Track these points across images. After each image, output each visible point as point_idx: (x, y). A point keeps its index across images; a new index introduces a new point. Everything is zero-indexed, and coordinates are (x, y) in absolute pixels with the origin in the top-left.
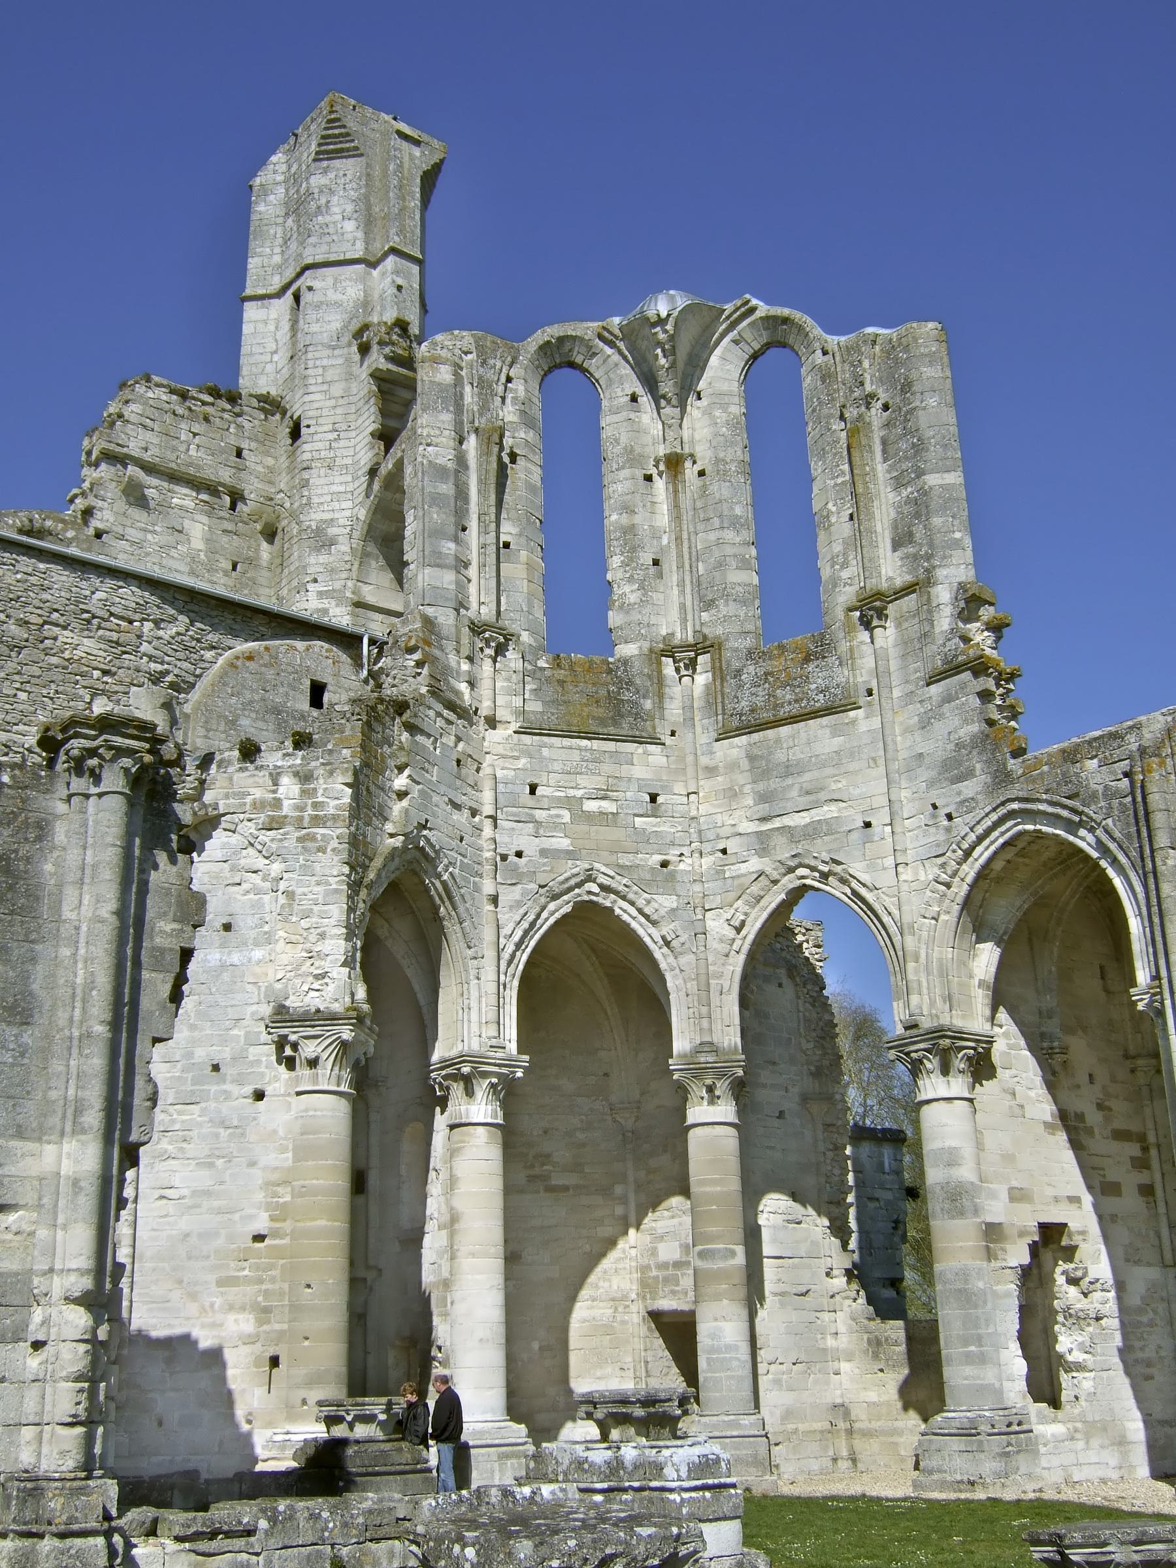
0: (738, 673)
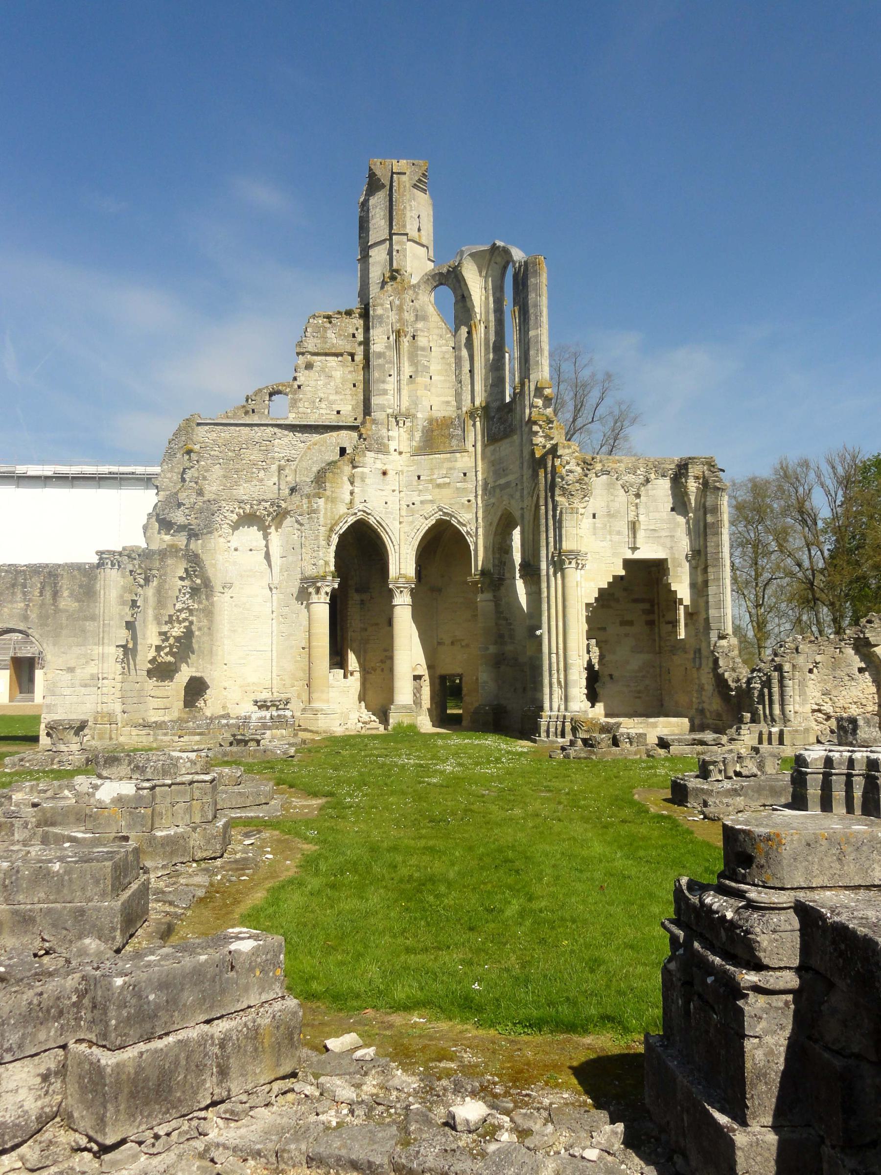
0: (494, 417)
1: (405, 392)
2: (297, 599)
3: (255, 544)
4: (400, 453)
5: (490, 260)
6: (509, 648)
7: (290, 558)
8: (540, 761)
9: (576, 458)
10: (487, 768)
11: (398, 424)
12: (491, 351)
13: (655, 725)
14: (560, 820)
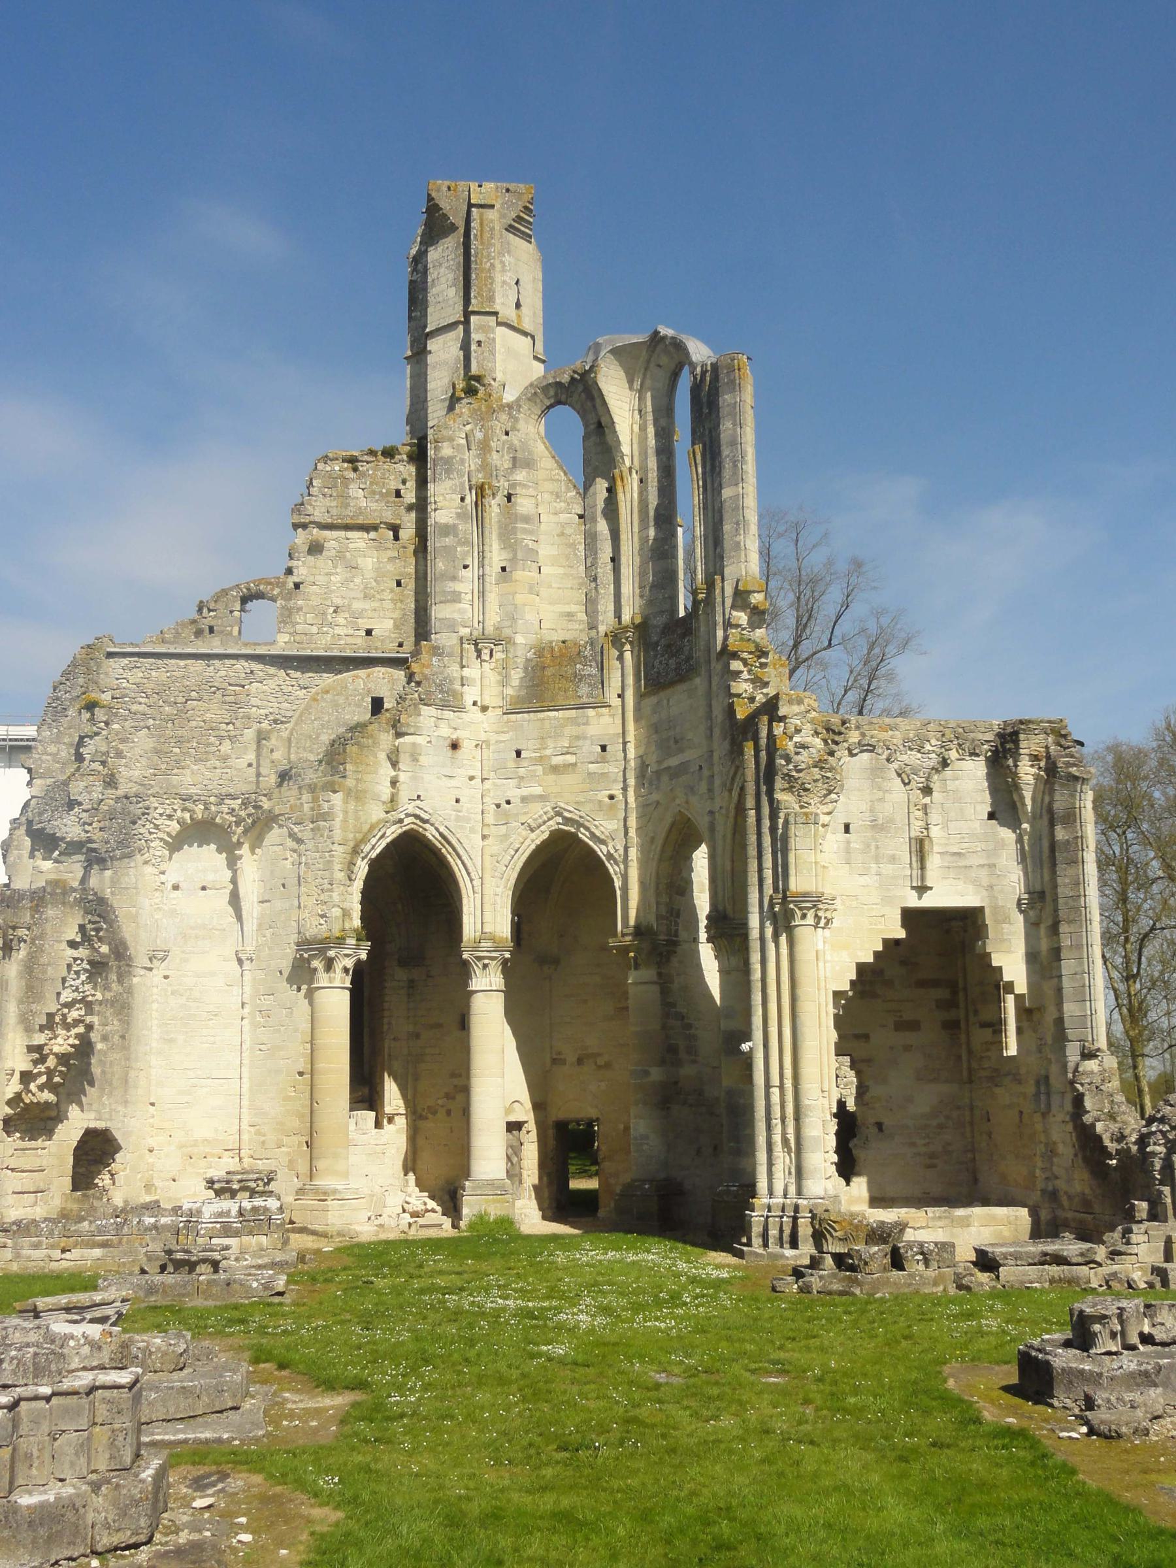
0: (657, 644)
1: (492, 597)
2: (290, 980)
3: (211, 877)
4: (484, 709)
5: (648, 361)
6: (687, 1071)
7: (278, 904)
8: (756, 1300)
9: (812, 722)
10: (657, 1319)
11: (479, 656)
12: (652, 523)
13: (965, 1223)
14: (812, 1443)
